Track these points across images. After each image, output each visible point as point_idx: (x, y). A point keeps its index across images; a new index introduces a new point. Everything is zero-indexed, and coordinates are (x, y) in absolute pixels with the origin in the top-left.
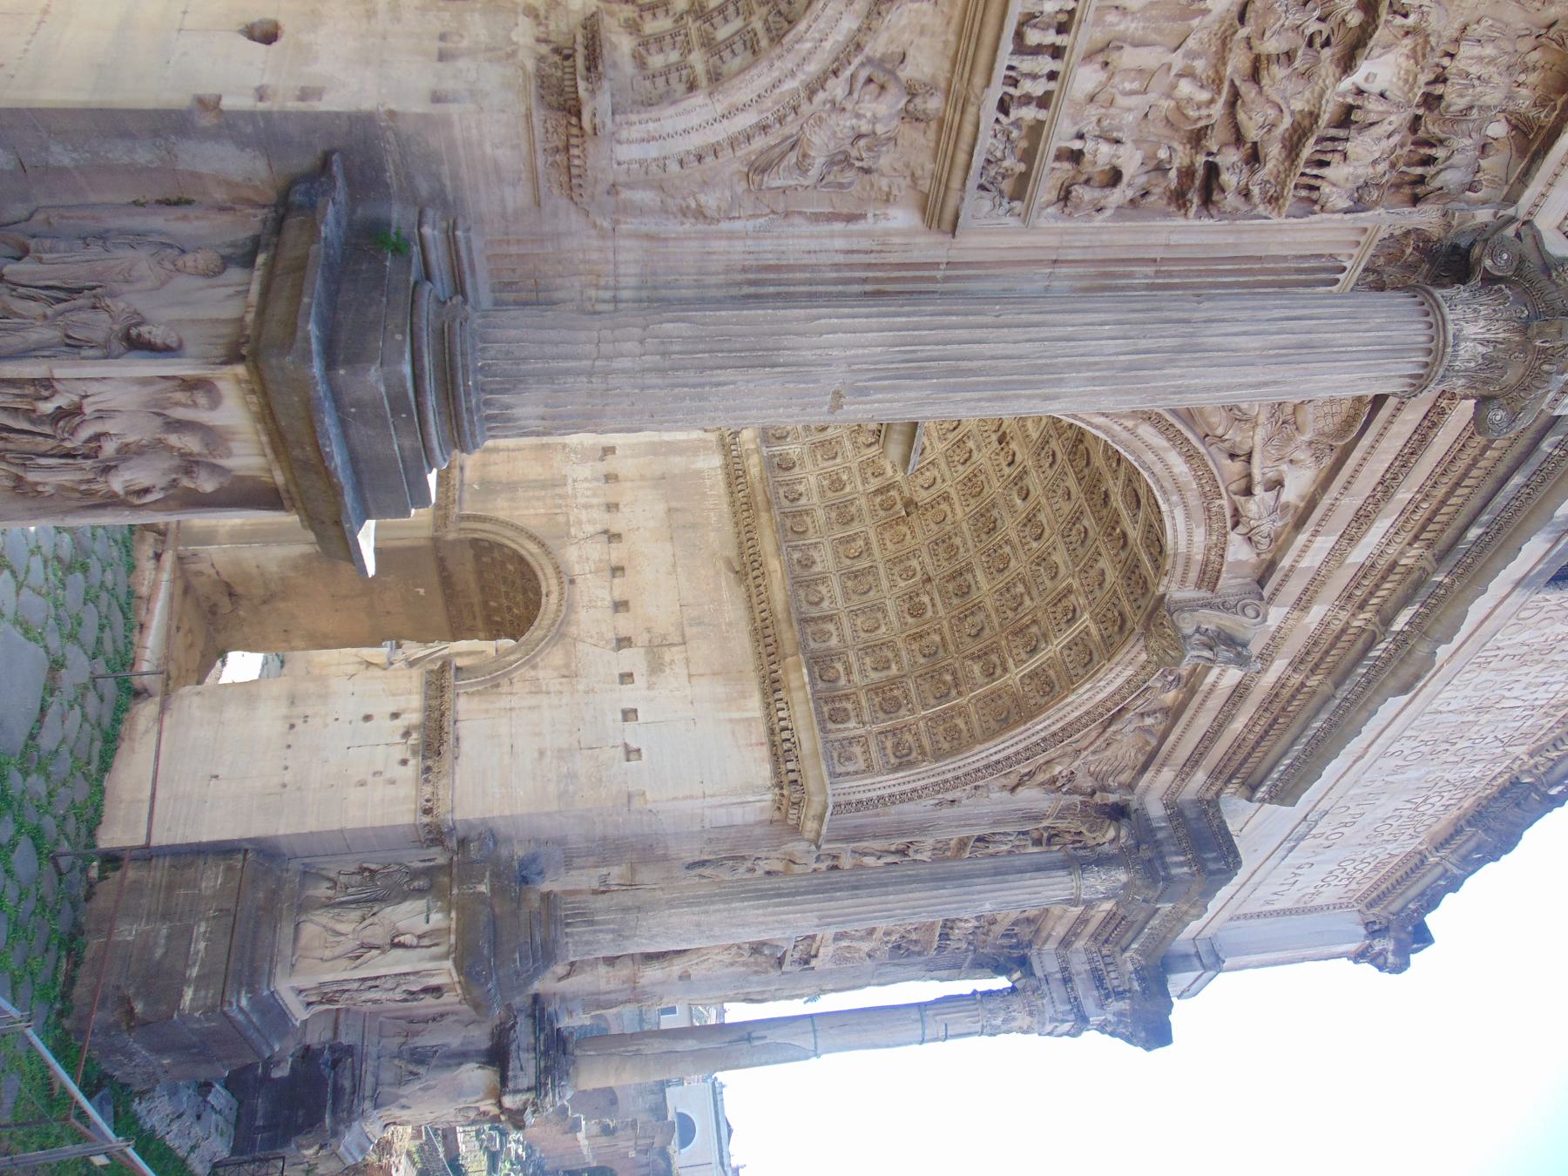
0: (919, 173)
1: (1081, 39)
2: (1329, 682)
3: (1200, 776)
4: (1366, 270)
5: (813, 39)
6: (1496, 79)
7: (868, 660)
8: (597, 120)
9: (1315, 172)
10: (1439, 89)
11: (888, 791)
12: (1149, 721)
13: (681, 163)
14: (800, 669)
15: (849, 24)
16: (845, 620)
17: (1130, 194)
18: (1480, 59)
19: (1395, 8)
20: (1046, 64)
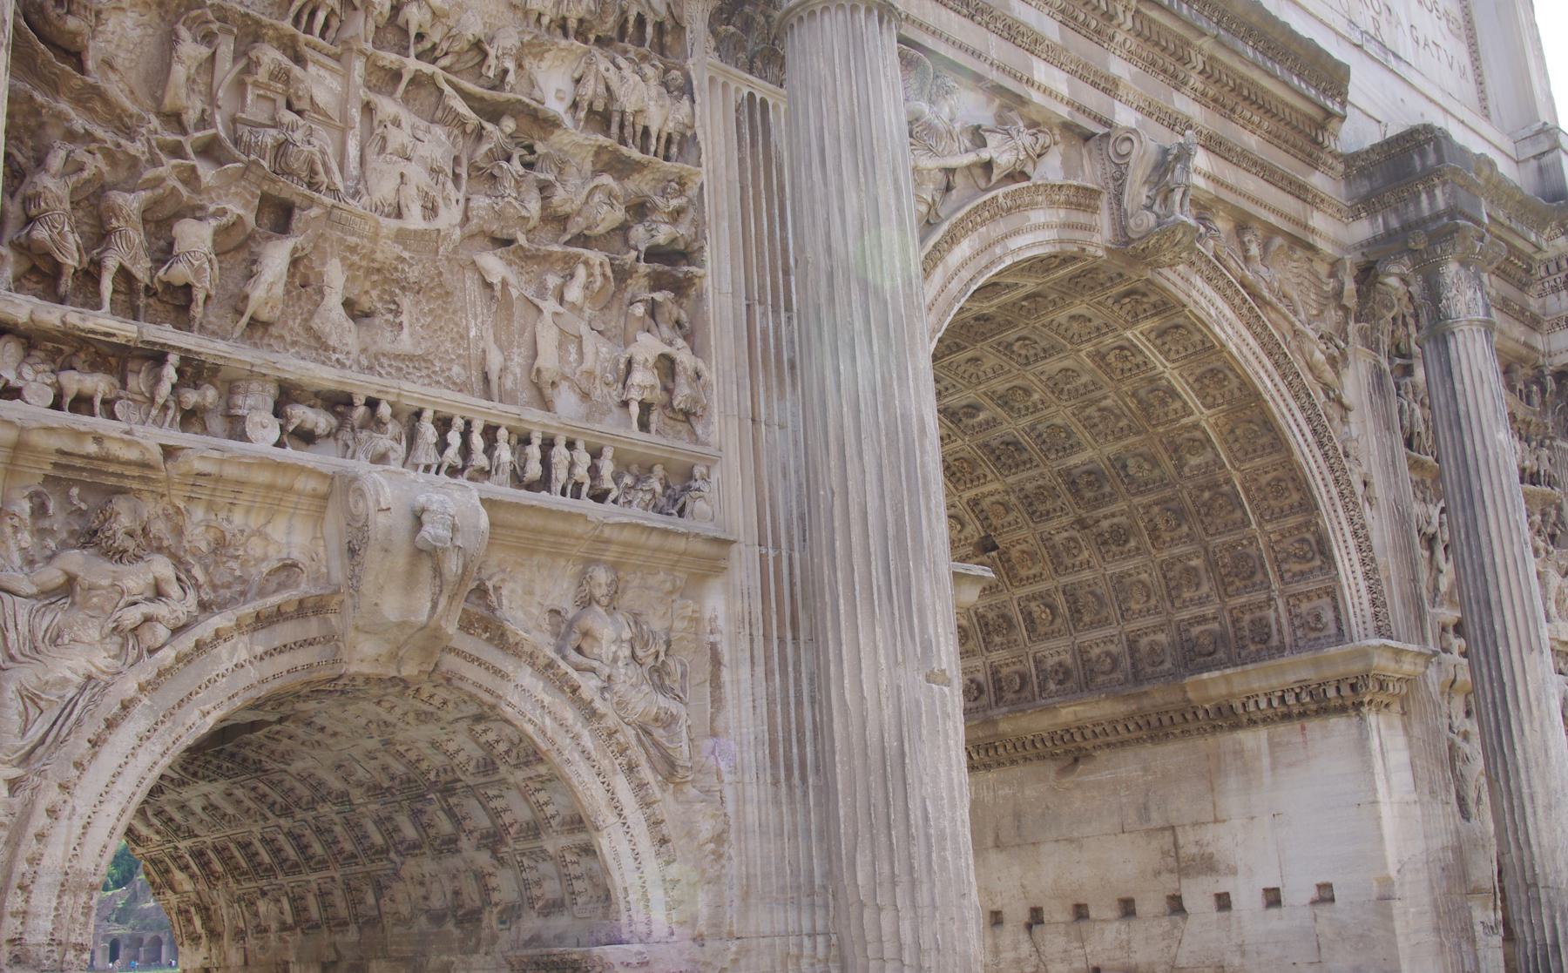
0: (668, 586)
1: (536, 420)
2: (1199, 43)
3: (1318, 181)
4: (751, 73)
7: (1186, 595)
8: (634, 961)
9: (654, 141)
10: (572, 24)
11: (1357, 567)
12: (1254, 250)
14: (1204, 683)
15: (526, 677)
16: (1134, 626)
17: (680, 342)
19: (497, 82)
20: (560, 454)
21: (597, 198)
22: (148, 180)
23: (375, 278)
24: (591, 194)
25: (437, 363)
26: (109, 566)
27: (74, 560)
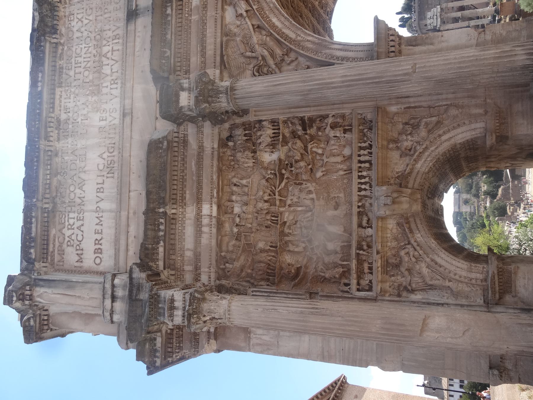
5: (428, 161)
6: (240, 159)
9: (276, 131)
10: (253, 154)
13: (464, 123)
15: (418, 166)
17: (326, 121)
18: (247, 163)
20: (362, 158)
21: (294, 147)
24: (294, 149)
26: (403, 263)
27: (403, 269)
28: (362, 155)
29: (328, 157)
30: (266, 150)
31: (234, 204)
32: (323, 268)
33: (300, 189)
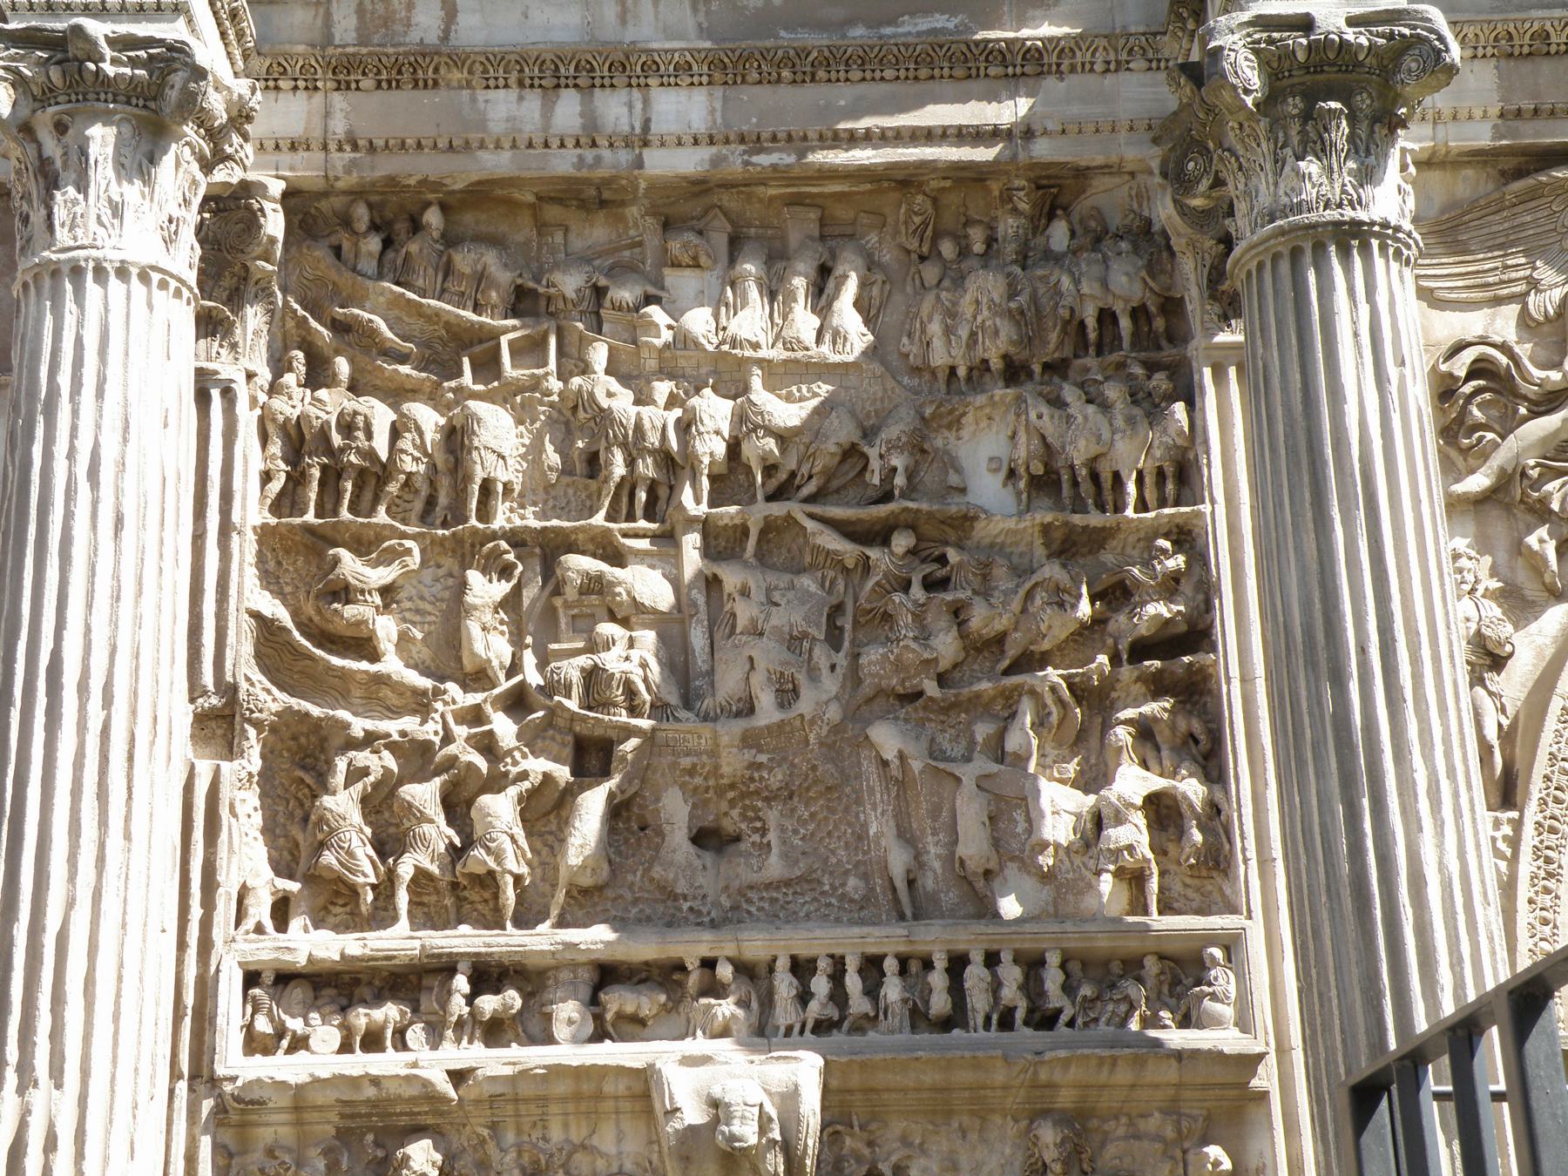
9: (1131, 488)
10: (996, 364)
18: (948, 331)
20: (975, 974)
22: (441, 763)
23: (731, 795)
24: (1029, 596)
25: (826, 880)
28: (994, 975)
29: (985, 784)
30: (1022, 438)
31: (718, 271)
32: (372, 778)
33: (805, 635)
